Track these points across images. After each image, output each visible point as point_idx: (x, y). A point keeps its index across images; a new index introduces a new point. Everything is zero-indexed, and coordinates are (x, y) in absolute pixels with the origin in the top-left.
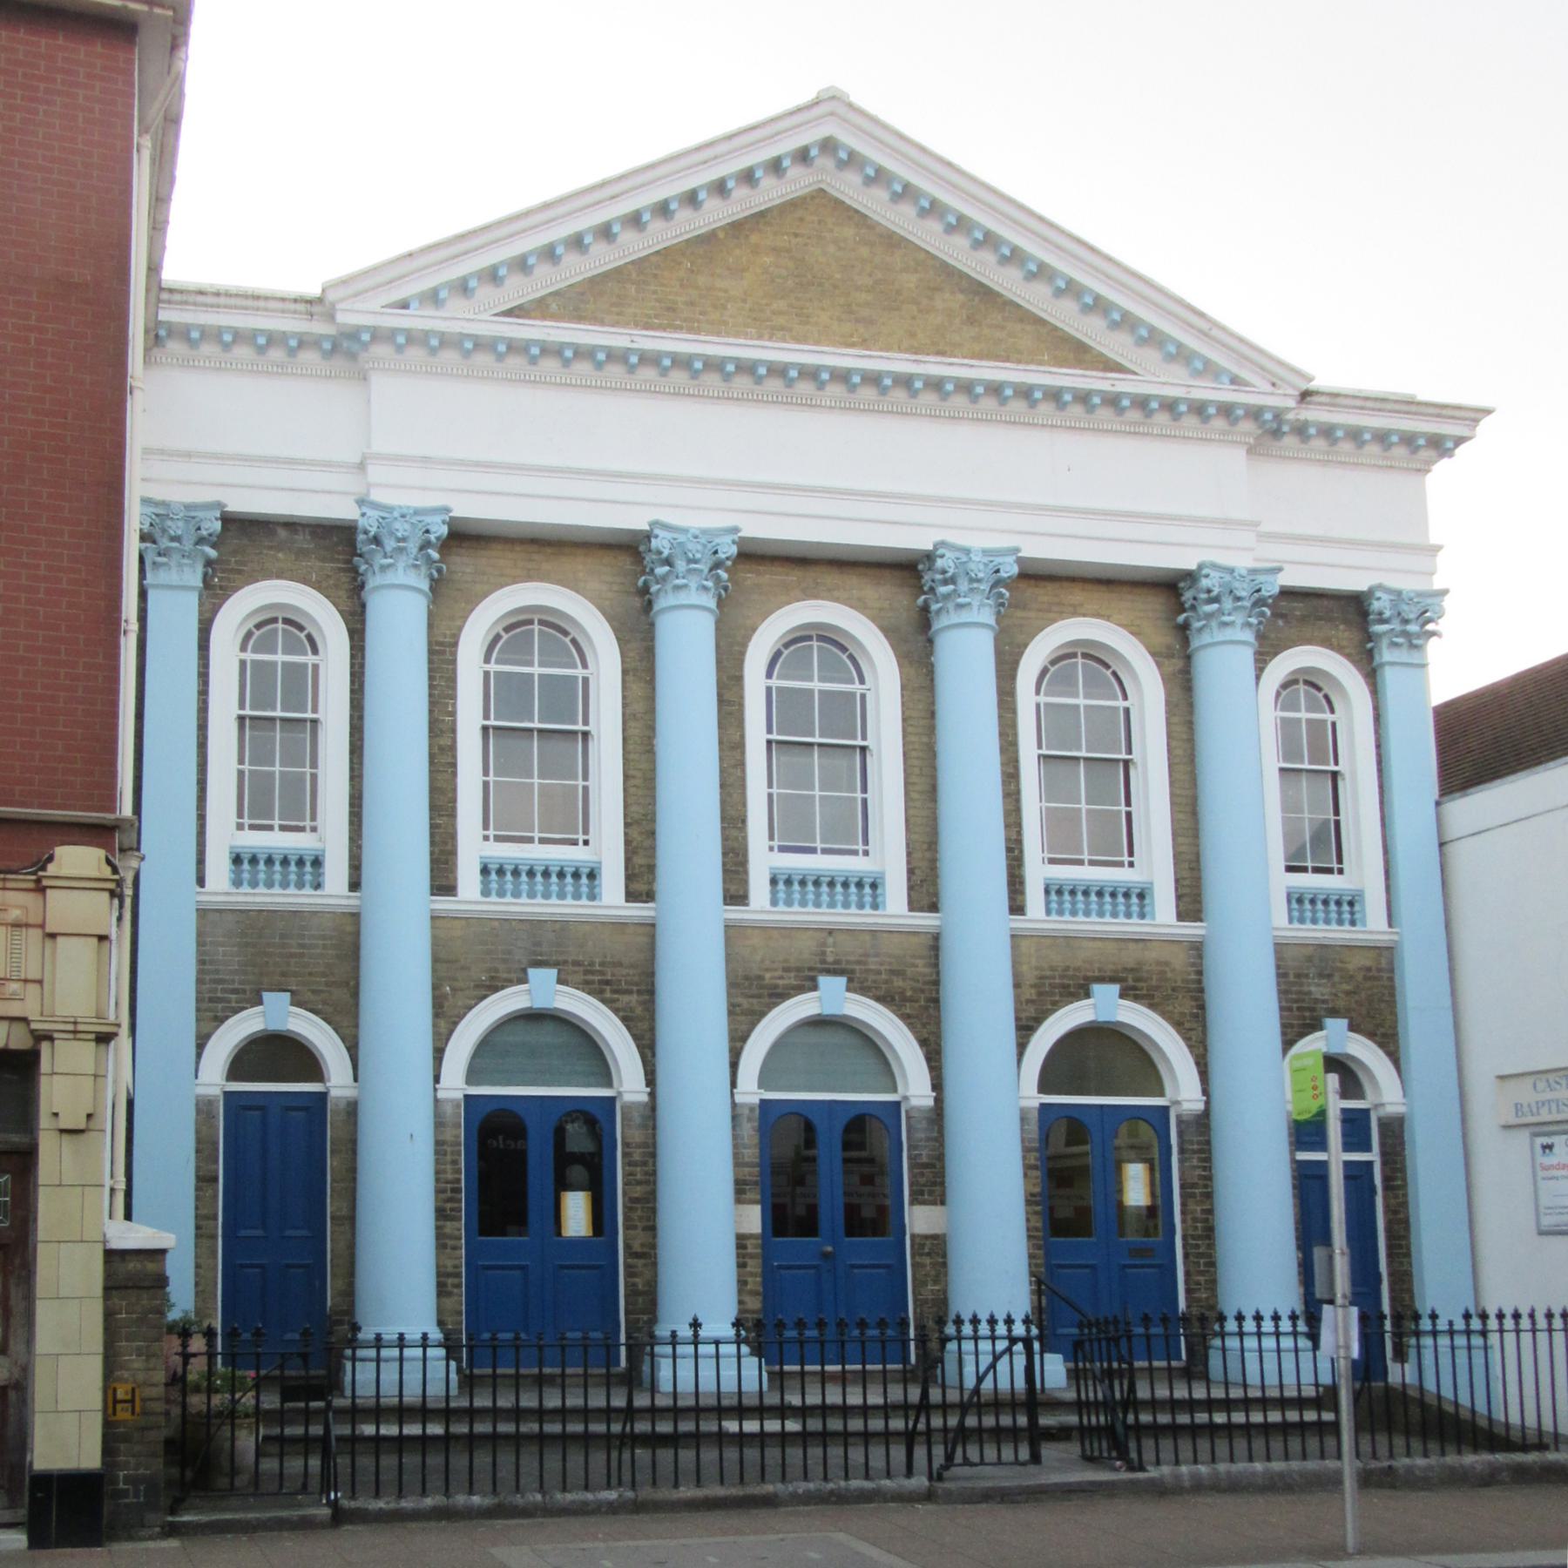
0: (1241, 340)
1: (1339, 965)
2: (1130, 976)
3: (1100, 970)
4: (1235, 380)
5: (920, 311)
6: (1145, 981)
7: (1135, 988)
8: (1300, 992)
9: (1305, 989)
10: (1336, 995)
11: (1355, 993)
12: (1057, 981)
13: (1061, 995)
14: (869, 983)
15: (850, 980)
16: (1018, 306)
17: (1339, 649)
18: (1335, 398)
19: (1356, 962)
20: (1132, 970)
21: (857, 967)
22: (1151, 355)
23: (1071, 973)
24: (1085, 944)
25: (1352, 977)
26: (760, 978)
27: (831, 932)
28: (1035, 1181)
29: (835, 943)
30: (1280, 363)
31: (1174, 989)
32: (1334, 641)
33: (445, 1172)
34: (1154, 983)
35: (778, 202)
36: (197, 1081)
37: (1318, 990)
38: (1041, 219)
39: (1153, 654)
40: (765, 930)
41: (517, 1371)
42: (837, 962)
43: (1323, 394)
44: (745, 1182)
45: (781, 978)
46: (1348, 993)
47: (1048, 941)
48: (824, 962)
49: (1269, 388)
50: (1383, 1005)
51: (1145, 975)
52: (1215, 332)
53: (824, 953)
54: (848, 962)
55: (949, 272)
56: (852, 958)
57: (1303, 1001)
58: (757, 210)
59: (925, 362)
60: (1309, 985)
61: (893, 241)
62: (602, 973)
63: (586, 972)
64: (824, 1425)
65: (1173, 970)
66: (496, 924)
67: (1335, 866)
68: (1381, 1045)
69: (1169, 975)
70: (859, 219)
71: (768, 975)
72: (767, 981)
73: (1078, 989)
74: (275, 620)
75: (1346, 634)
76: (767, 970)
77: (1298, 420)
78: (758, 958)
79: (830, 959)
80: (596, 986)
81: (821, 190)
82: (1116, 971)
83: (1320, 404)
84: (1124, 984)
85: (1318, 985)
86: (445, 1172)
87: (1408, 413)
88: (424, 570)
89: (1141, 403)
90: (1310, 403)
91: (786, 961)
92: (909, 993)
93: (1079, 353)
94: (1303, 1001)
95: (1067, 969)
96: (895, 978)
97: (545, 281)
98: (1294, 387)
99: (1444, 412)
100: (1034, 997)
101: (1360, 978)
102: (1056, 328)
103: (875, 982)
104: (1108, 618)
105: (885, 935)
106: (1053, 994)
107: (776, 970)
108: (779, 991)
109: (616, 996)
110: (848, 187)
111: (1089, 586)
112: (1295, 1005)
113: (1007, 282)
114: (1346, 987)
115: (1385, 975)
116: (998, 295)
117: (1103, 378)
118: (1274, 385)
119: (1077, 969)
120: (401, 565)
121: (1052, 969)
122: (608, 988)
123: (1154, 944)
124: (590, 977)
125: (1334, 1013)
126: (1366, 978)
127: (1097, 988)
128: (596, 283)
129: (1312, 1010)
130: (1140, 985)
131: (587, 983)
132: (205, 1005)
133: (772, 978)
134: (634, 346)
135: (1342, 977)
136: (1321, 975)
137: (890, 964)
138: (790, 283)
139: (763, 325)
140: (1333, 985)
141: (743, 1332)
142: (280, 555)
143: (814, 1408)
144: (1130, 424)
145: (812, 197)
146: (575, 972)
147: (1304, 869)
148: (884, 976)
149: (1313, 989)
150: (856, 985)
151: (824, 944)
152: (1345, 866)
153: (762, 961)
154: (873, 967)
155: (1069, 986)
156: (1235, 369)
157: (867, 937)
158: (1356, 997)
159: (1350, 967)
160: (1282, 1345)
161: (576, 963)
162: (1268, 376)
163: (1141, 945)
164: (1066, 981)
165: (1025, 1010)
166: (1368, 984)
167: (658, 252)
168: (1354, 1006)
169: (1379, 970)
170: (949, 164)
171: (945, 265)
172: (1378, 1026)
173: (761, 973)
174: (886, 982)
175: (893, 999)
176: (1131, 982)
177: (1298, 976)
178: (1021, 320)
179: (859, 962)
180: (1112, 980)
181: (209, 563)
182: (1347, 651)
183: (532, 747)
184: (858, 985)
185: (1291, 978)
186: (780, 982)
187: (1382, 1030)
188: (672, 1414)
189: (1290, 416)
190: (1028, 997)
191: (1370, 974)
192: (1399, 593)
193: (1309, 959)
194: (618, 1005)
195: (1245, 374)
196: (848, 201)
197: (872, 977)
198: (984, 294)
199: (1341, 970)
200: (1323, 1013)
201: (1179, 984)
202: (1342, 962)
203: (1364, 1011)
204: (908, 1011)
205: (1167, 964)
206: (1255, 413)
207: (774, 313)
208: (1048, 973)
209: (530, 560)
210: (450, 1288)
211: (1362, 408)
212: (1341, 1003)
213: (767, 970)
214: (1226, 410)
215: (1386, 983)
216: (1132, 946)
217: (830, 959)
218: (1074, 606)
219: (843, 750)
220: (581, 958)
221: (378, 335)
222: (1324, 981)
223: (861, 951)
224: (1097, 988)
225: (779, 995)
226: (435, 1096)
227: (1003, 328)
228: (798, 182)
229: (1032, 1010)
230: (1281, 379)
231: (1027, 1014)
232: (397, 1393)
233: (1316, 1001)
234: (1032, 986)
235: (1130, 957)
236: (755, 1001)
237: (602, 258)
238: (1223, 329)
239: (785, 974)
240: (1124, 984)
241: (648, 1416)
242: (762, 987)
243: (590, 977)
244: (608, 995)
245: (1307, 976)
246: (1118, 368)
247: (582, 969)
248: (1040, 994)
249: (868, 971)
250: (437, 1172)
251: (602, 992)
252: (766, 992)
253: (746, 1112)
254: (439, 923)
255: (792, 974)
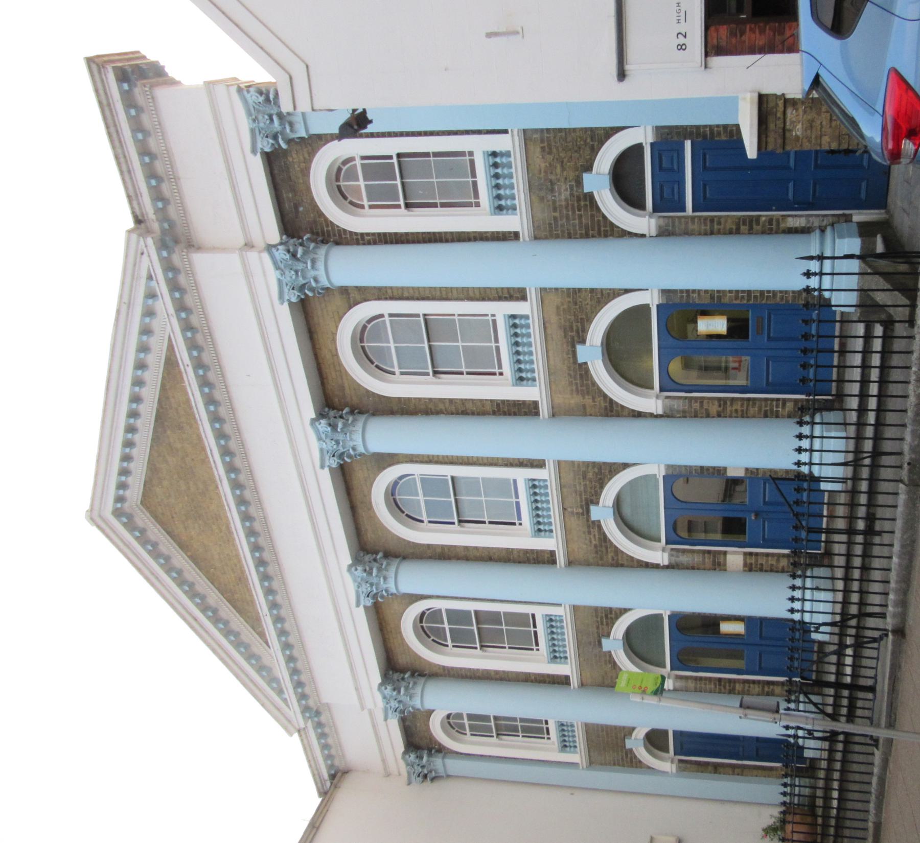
0: (123, 283)
1: (543, 174)
2: (570, 334)
3: (568, 354)
4: (150, 278)
5: (187, 456)
6: (572, 323)
7: (578, 332)
8: (567, 207)
9: (563, 203)
10: (566, 179)
11: (562, 162)
12: (579, 382)
13: (587, 380)
14: (593, 491)
15: (592, 502)
16: (159, 399)
17: (308, 162)
18: (132, 197)
19: (540, 162)
20: (565, 332)
21: (584, 497)
22: (156, 324)
23: (572, 373)
24: (552, 362)
25: (550, 164)
26: (596, 546)
27: (564, 509)
28: (711, 404)
29: (571, 508)
30: (126, 256)
31: (576, 304)
32: (303, 165)
33: (711, 689)
34: (573, 318)
35: (159, 527)
36: (670, 772)
37: (563, 194)
38: (105, 411)
39: (350, 308)
40: (568, 542)
41: (815, 671)
42: (582, 507)
43: (132, 208)
44: (714, 561)
45: (595, 535)
46: (563, 169)
47: (553, 387)
48: (582, 514)
49: (145, 256)
50: (569, 139)
51: (568, 324)
52: (126, 299)
53: (577, 513)
54: (581, 501)
55: (156, 439)
56: (579, 499)
57: (573, 205)
58: (168, 537)
59: (219, 476)
60: (560, 200)
61: (153, 469)
62: (602, 618)
63: (602, 624)
64: (856, 580)
65: (563, 304)
66: (581, 659)
67: (467, 158)
68: (602, 143)
69: (565, 307)
70: (148, 485)
71: (594, 542)
72: (597, 543)
73: (583, 371)
74: (449, 723)
75: (294, 156)
76: (591, 542)
77: (157, 219)
78: (585, 546)
79: (580, 511)
80: (609, 621)
81: (141, 503)
82: (568, 343)
83: (140, 208)
84: (576, 338)
85: (560, 194)
86: (711, 689)
87: (117, 131)
88: (412, 691)
89: (187, 327)
90: (143, 215)
91: (584, 533)
92: (596, 470)
93: (171, 363)
94: (573, 205)
95: (570, 375)
96: (587, 477)
97: (248, 634)
98: (138, 242)
99: (105, 102)
100: (590, 397)
101: (551, 157)
102: (163, 378)
103: (591, 488)
104: (334, 334)
105: (562, 481)
106: (587, 385)
107: (590, 538)
108: (602, 537)
109: (613, 613)
110: (134, 493)
111: (317, 346)
112: (577, 213)
113: (148, 410)
114: (559, 170)
115: (546, 135)
116: (158, 411)
117: (186, 373)
118: (142, 254)
119: (569, 368)
120: (412, 703)
121: (571, 384)
122: (609, 616)
123: (545, 316)
124: (605, 623)
125: (579, 182)
126: (550, 153)
127: (580, 360)
128: (241, 612)
129: (579, 199)
130: (575, 328)
131: (607, 624)
132: (634, 765)
133: (595, 540)
134: (268, 614)
135: (551, 173)
136: (552, 190)
137: (579, 479)
138: (200, 522)
139: (228, 538)
140: (559, 180)
141: (799, 573)
142: (418, 725)
143: (844, 597)
144: (206, 339)
145: (147, 508)
146: (603, 629)
147: (475, 184)
148: (588, 483)
149: (563, 197)
150: (594, 498)
151: (572, 513)
152: (467, 149)
153: (587, 545)
154: (582, 488)
155: (581, 375)
156: (143, 281)
157: (565, 490)
158: (565, 160)
159: (543, 165)
160: (829, 271)
161: (598, 628)
162: (138, 260)
163: (547, 325)
164: (578, 376)
165: (600, 403)
166: (554, 150)
167: (212, 583)
168: (572, 164)
169: (542, 141)
170: (98, 461)
171: (153, 440)
172: (586, 144)
173: (593, 546)
174: (591, 481)
175: (600, 479)
176: (574, 334)
177: (555, 210)
178: (167, 398)
179: (581, 495)
180: (574, 347)
181: (430, 754)
182: (306, 156)
183: (486, 628)
184: (593, 498)
185: (557, 214)
186: (597, 536)
187: (589, 140)
188: (840, 676)
189: (156, 226)
190: (591, 401)
191: (547, 150)
192: (252, 131)
193: (542, 199)
194: (618, 614)
195: (144, 274)
196: (141, 490)
197: (589, 490)
198: (160, 418)
199: (546, 172)
200: (580, 190)
201: (571, 300)
202: (540, 173)
203: (576, 155)
204: (607, 471)
205: (558, 308)
206: (169, 267)
207: (221, 532)
208: (574, 388)
209: (391, 632)
210: (770, 690)
211: (129, 172)
212: (572, 175)
213: (591, 542)
214: (174, 286)
215: (552, 135)
216: (549, 331)
217: (580, 511)
218: (333, 356)
219: (456, 485)
220: (595, 626)
221: (305, 709)
222: (556, 187)
223: (574, 495)
224: (580, 360)
225: (604, 539)
226: (670, 567)
227: (177, 409)
228: (143, 519)
229: (599, 399)
230: (137, 251)
231: (602, 402)
232: (820, 751)
233: (572, 195)
234: (584, 398)
235: (557, 334)
236: (609, 550)
237: (226, 611)
238: (121, 297)
239: (593, 534)
240: (576, 338)
241: (841, 667)
242: (601, 546)
243: (605, 623)
244: (613, 616)
245: (554, 202)
246: (171, 348)
247: (600, 626)
248: (588, 393)
249: (585, 492)
250: (711, 692)
251: (611, 618)
252: (603, 544)
253: (673, 559)
254: (584, 681)
255: (592, 530)
